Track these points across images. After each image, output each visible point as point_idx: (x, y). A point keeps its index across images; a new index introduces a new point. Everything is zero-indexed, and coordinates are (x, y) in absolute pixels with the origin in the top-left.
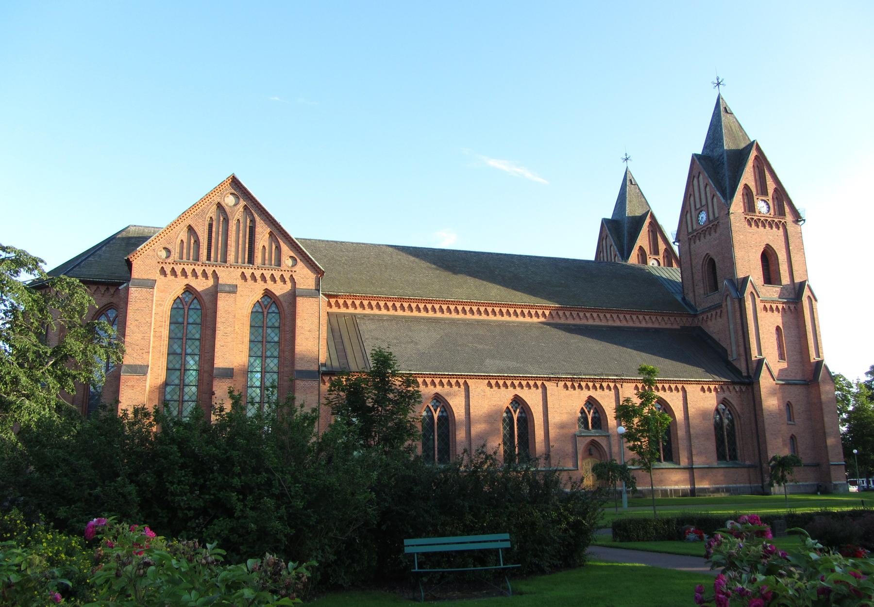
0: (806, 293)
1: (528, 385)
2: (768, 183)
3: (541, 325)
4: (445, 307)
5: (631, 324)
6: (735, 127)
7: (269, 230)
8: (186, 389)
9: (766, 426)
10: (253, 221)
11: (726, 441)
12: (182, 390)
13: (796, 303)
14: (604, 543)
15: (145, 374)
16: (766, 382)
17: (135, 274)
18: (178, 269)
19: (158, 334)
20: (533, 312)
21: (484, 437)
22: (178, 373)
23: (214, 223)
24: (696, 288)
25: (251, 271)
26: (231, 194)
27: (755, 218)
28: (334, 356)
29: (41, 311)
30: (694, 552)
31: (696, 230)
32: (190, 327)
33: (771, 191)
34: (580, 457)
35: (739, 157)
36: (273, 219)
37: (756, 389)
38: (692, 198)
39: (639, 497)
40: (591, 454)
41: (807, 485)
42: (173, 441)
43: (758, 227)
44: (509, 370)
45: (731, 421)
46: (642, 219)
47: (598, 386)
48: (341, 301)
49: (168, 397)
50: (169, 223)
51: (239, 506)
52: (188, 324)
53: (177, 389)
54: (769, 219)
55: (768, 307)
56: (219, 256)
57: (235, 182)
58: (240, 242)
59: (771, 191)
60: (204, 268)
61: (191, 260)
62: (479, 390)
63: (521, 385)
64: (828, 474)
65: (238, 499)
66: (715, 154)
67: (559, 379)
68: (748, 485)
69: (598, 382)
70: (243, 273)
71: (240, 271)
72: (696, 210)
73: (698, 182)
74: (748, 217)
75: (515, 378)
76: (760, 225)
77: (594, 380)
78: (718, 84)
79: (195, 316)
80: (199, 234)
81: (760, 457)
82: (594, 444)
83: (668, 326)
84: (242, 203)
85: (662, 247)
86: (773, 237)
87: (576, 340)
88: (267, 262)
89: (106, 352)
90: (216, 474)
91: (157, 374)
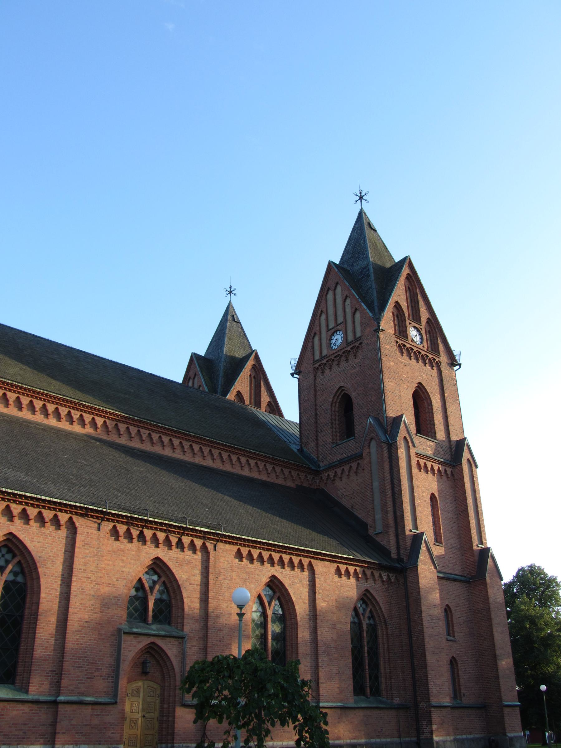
0: (466, 455)
1: (40, 518)
2: (421, 309)
5: (228, 468)
9: (427, 640)
27: (408, 346)
31: (326, 356)
38: (323, 317)
40: (145, 673)
41: (472, 740)
45: (373, 629)
47: (174, 540)
54: (423, 353)
55: (422, 465)
63: (24, 515)
64: (501, 721)
66: (356, 268)
67: (103, 516)
69: (176, 532)
72: (328, 330)
73: (335, 295)
77: (168, 529)
82: (153, 652)
83: (280, 481)
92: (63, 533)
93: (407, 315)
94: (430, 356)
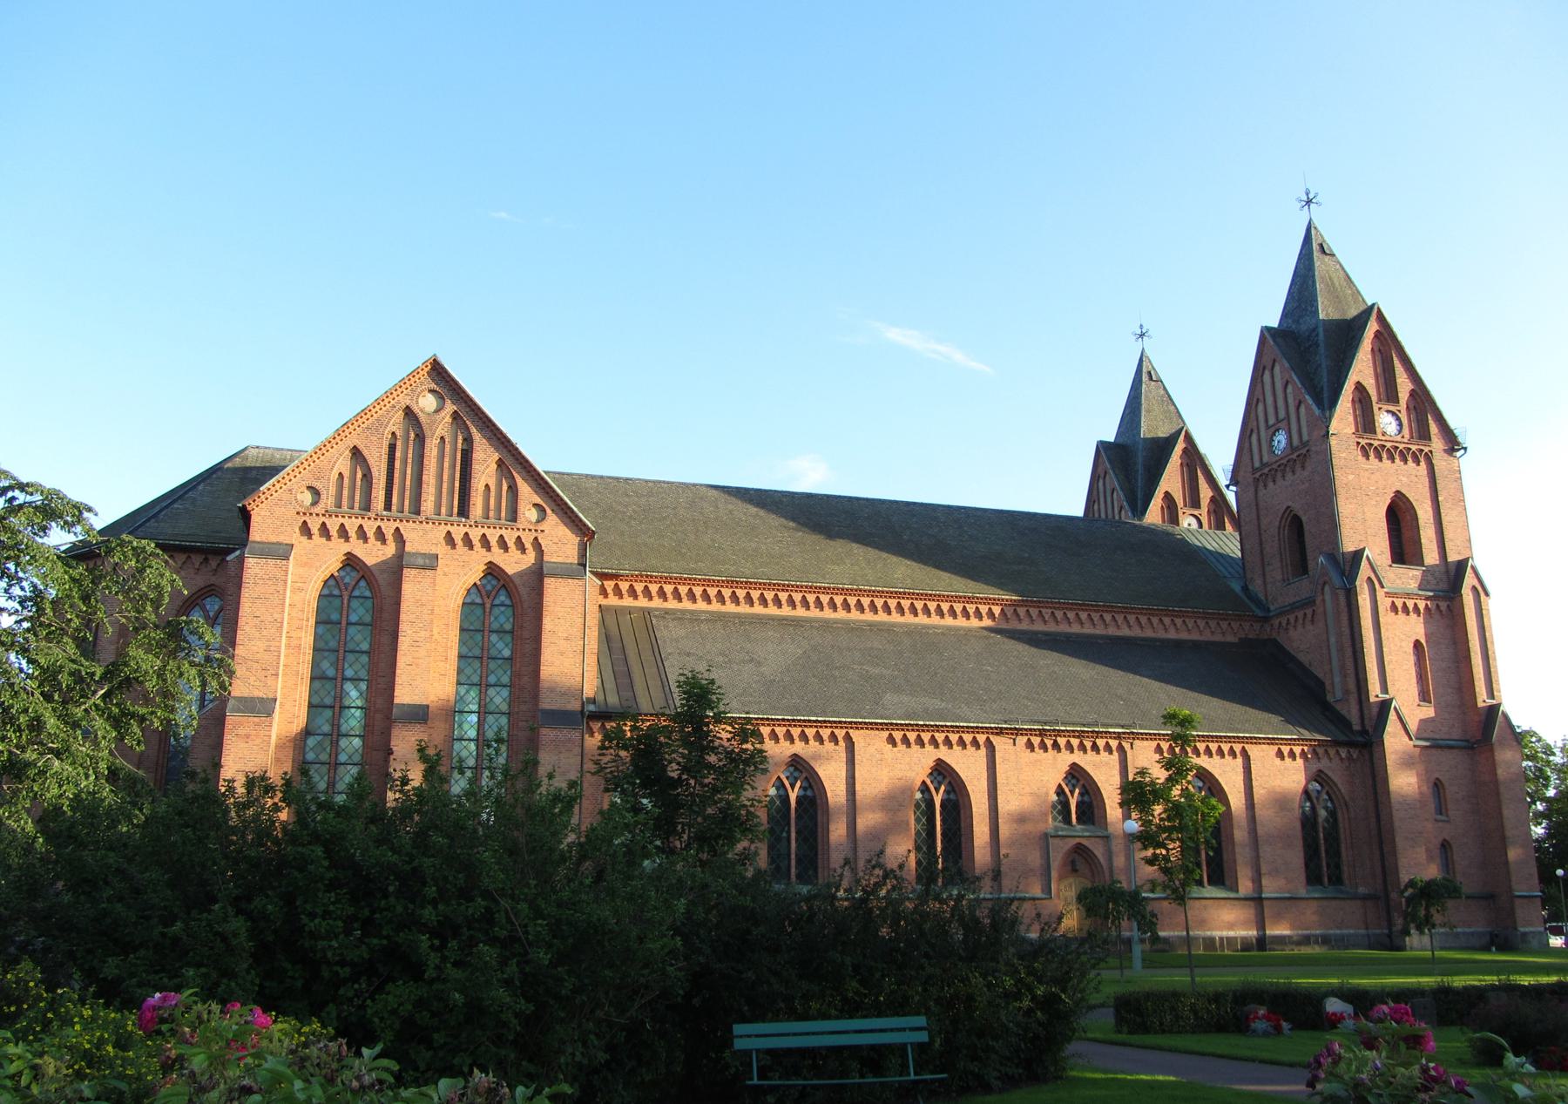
0: (1469, 580)
1: (961, 742)
2: (1399, 381)
3: (986, 633)
4: (811, 598)
5: (1149, 633)
6: (1338, 281)
7: (496, 456)
8: (343, 743)
9: (1397, 824)
10: (468, 440)
11: (1323, 848)
12: (335, 744)
13: (1451, 599)
14: (1098, 1035)
15: (270, 714)
16: (1395, 742)
17: (257, 533)
18: (333, 528)
19: (294, 643)
20: (971, 608)
21: (879, 836)
22: (329, 713)
23: (399, 443)
24: (1268, 569)
25: (463, 530)
26: (431, 391)
27: (1376, 443)
28: (610, 685)
29: (86, 598)
30: (1265, 1055)
32: (352, 630)
33: (1404, 395)
34: (1054, 874)
35: (1347, 334)
36: (505, 437)
37: (1376, 755)
38: (1260, 407)
39: (1164, 951)
40: (1075, 870)
41: (1472, 934)
42: (316, 838)
43: (1381, 460)
44: (927, 714)
45: (1332, 813)
46: (1170, 442)
47: (1088, 744)
48: (624, 586)
49: (310, 756)
50: (318, 443)
51: (434, 959)
52: (349, 624)
53: (327, 743)
54: (1401, 446)
56: (407, 503)
57: (437, 370)
58: (445, 477)
59: (1404, 395)
60: (378, 523)
61: (356, 510)
62: (872, 750)
63: (948, 742)
64: (1511, 913)
65: (432, 947)
66: (1304, 327)
67: (1018, 732)
68: (1363, 932)
69: (1088, 738)
70: (449, 533)
71: (443, 529)
72: (1268, 427)
73: (1272, 377)
74: (1363, 442)
75: (938, 728)
76: (1384, 456)
78: (1309, 202)
79: (362, 610)
80: (372, 461)
81: (1385, 881)
82: (1080, 850)
83: (1218, 638)
84: (450, 407)
85: (1206, 493)
86: (1409, 479)
87: (1049, 660)
88: (492, 514)
89: (201, 674)
90: (392, 900)
91: (290, 715)
92: (983, 751)
93: (1374, 398)
94: (1414, 448)
